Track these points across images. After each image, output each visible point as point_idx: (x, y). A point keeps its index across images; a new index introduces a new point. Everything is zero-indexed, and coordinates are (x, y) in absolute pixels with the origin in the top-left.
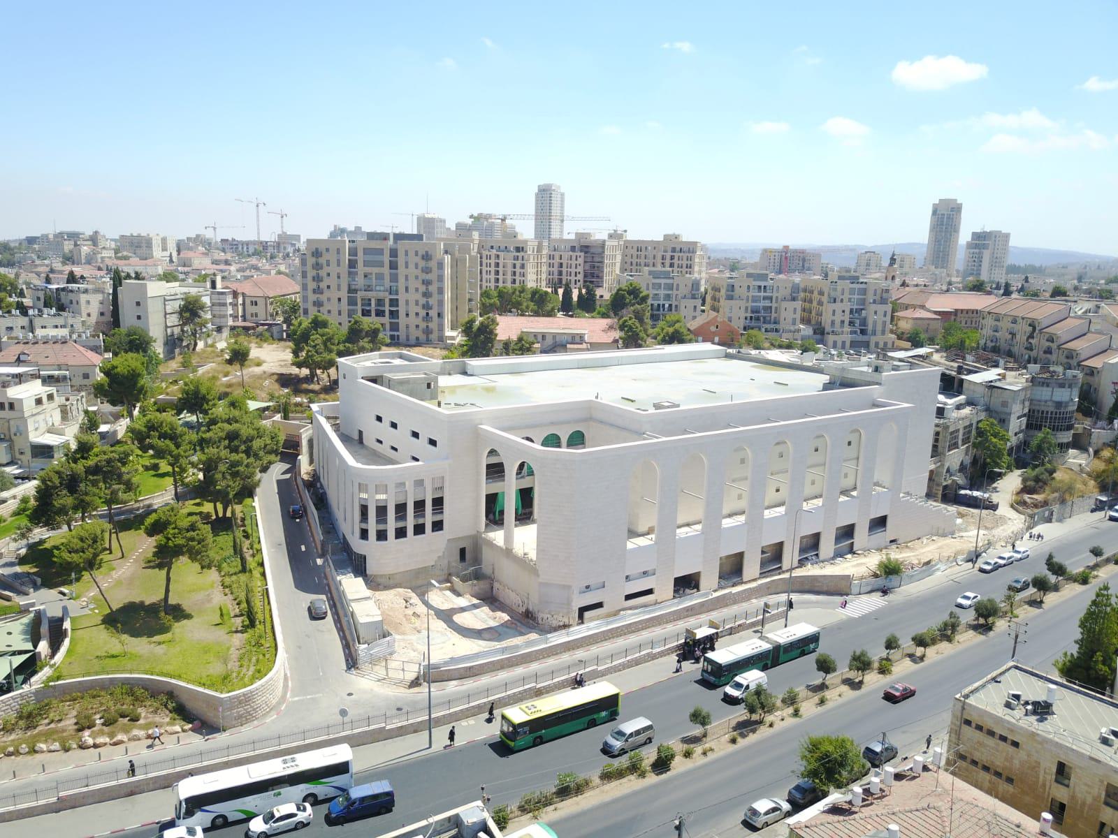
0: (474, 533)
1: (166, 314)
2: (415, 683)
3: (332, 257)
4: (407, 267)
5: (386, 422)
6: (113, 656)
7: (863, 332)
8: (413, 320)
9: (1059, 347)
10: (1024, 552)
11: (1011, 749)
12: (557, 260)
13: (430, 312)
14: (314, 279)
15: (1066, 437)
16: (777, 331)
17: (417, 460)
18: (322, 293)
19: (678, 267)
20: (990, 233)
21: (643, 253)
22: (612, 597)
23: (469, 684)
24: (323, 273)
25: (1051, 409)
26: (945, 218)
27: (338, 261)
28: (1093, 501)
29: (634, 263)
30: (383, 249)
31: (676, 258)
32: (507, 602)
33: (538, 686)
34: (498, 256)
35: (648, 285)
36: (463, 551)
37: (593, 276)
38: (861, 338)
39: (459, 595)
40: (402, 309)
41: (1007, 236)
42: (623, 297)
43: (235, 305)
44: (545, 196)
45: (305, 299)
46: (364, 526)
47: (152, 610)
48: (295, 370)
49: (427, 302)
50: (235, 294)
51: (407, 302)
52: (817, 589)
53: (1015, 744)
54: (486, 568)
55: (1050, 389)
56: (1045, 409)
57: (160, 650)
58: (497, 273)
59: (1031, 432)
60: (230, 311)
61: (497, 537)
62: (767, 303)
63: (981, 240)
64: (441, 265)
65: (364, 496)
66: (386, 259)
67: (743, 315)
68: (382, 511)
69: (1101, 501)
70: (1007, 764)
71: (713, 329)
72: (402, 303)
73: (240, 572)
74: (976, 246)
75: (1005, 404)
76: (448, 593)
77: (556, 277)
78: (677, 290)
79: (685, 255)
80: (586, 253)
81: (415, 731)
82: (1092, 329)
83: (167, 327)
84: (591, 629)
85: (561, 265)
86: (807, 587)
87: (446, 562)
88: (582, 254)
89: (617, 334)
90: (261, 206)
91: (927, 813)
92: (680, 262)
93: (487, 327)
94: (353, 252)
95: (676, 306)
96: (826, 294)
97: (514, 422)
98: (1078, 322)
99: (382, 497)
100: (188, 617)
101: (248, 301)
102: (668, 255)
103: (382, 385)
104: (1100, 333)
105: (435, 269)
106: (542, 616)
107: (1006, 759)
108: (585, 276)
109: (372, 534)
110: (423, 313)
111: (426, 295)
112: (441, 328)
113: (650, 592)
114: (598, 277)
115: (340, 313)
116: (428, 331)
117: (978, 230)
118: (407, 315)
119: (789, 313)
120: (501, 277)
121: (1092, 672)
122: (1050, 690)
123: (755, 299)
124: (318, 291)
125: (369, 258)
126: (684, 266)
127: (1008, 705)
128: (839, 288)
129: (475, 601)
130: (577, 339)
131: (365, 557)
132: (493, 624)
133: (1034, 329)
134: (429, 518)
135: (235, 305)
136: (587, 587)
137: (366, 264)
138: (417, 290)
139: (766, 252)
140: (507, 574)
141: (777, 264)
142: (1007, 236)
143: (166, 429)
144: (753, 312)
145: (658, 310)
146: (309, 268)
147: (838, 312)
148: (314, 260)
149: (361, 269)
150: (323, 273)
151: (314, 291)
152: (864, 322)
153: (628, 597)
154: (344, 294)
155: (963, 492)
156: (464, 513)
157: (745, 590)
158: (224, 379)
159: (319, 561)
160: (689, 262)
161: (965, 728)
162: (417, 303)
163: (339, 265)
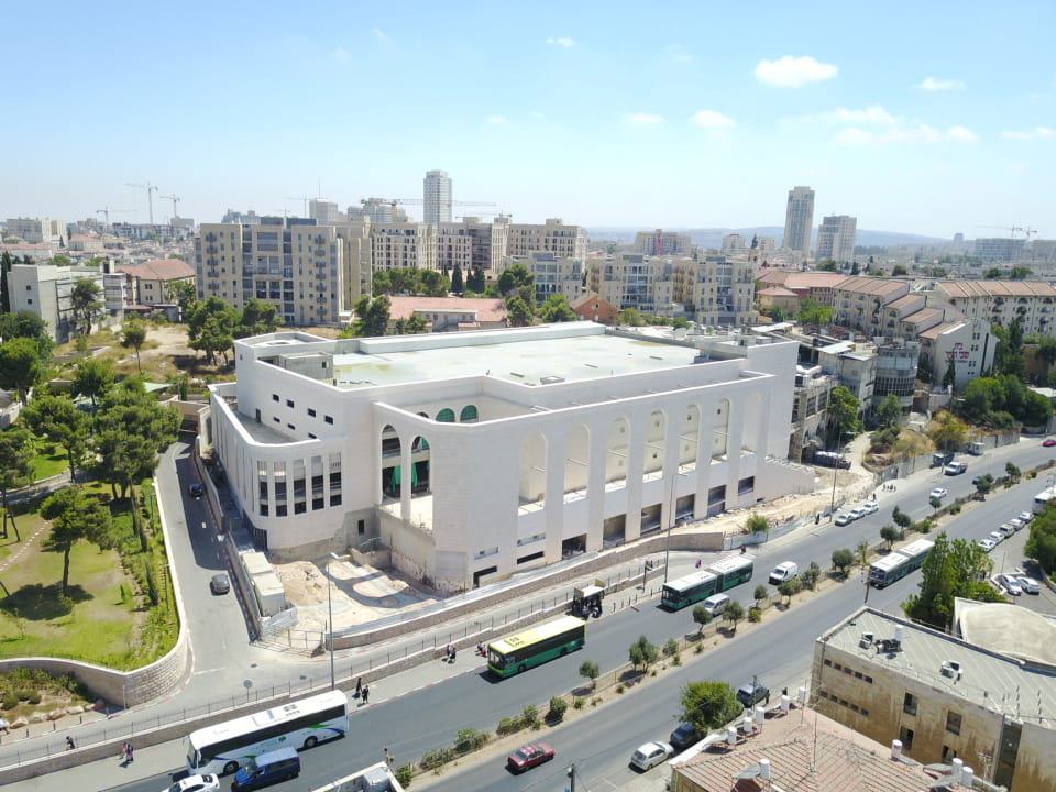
0: (372, 506)
2: (318, 652)
3: (227, 241)
4: (301, 250)
5: (283, 401)
6: (11, 640)
7: (730, 309)
8: (307, 302)
9: (900, 321)
11: (866, 685)
12: (446, 243)
13: (325, 294)
14: (208, 262)
15: (908, 401)
16: (652, 309)
17: (314, 437)
18: (217, 276)
20: (840, 218)
21: (527, 237)
22: (506, 562)
23: (371, 650)
24: (218, 257)
25: (895, 377)
26: (800, 203)
28: (931, 458)
30: (276, 234)
31: (558, 241)
32: (406, 570)
36: (361, 524)
37: (481, 259)
38: (727, 314)
39: (358, 565)
40: (296, 292)
41: (854, 221)
42: (510, 278)
43: (129, 289)
44: (434, 182)
45: (200, 283)
46: (264, 502)
47: (51, 592)
48: (192, 352)
49: (321, 284)
50: (129, 278)
51: (301, 284)
52: (694, 547)
53: (869, 680)
54: (384, 539)
55: (893, 359)
56: (890, 377)
57: (59, 632)
58: (389, 255)
59: (878, 398)
60: (124, 294)
61: (395, 509)
62: (642, 283)
63: (832, 224)
64: (334, 249)
65: (263, 473)
66: (280, 243)
67: (620, 294)
68: (281, 487)
69: (938, 458)
70: (862, 698)
71: (594, 308)
73: (141, 551)
74: (828, 229)
75: (855, 373)
76: (348, 564)
77: (446, 259)
80: (474, 236)
82: (929, 303)
85: (450, 248)
86: (684, 545)
87: (344, 538)
88: (470, 238)
89: (505, 313)
90: (154, 191)
91: (794, 747)
93: (380, 307)
94: (247, 236)
96: (696, 273)
97: (410, 398)
98: (915, 298)
99: (282, 474)
100: (89, 597)
101: (142, 285)
102: (551, 238)
103: (278, 365)
104: (935, 307)
106: (440, 582)
107: (862, 693)
108: (474, 258)
109: (272, 510)
111: (320, 276)
112: (335, 309)
113: (540, 555)
114: (486, 259)
115: (235, 295)
116: (322, 312)
117: (829, 215)
118: (302, 296)
119: (662, 291)
120: (392, 259)
121: (933, 612)
122: (898, 630)
123: (632, 280)
124: (213, 274)
125: (264, 242)
126: (566, 249)
127: (862, 645)
128: (708, 269)
129: (375, 571)
130: (468, 318)
131: (266, 532)
132: (392, 592)
133: (879, 306)
134: (327, 493)
135: (129, 289)
136: (482, 553)
137: (260, 248)
138: (311, 272)
139: (640, 234)
140: (404, 545)
141: (651, 246)
142: (854, 221)
143: (61, 412)
144: (629, 291)
145: (543, 290)
146: (203, 251)
147: (708, 291)
148: (208, 244)
149: (255, 252)
150: (218, 257)
151: (209, 275)
152: (730, 300)
153: (520, 561)
154: (239, 277)
155: (820, 453)
156: (362, 488)
158: (120, 362)
159: (220, 538)
160: (570, 245)
161: (826, 668)
162: (311, 285)
163: (233, 249)
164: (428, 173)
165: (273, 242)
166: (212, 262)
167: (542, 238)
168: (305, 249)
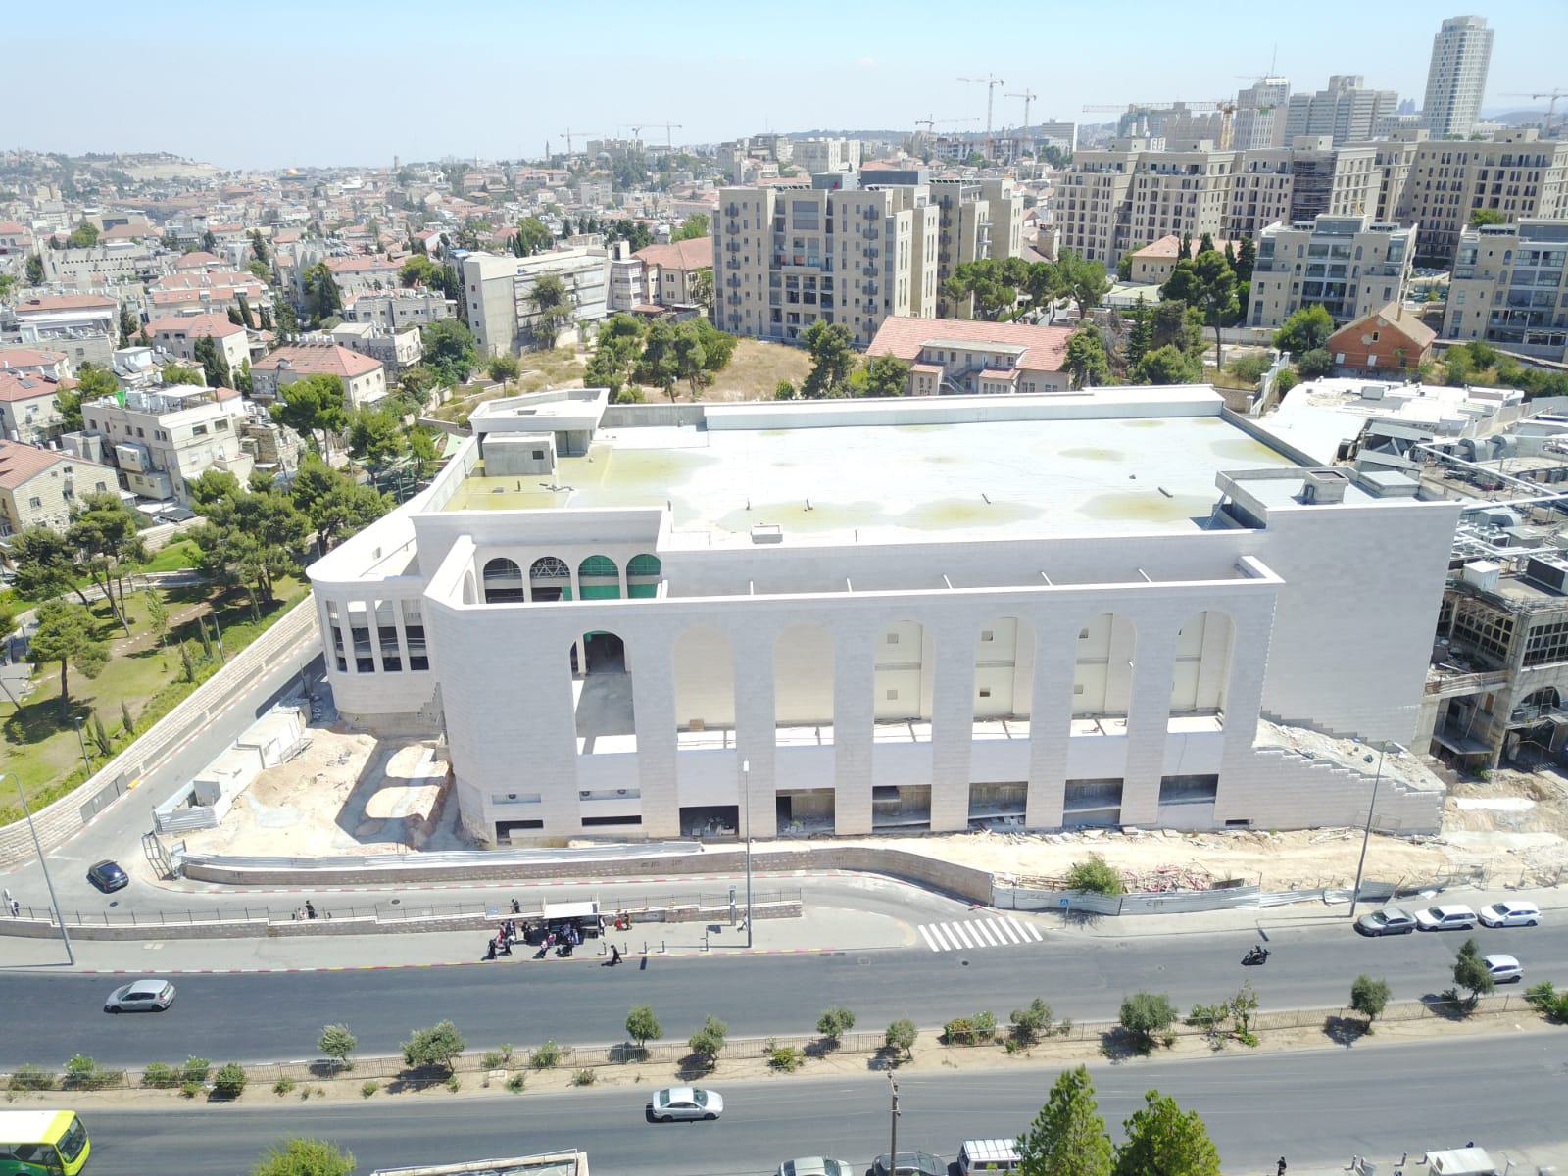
1: (516, 300)
4: (845, 230)
8: (852, 311)
10: (1513, 914)
12: (1250, 187)
13: (874, 298)
18: (738, 268)
19: (1509, 193)
21: (1452, 166)
22: (562, 814)
24: (739, 239)
27: (758, 220)
29: (1434, 185)
31: (1507, 176)
33: (273, 924)
34: (1156, 182)
35: (1301, 248)
43: (643, 281)
45: (719, 273)
49: (871, 284)
50: (645, 266)
52: (933, 880)
60: (635, 288)
64: (890, 225)
67: (1486, 308)
71: (1367, 340)
72: (837, 284)
73: (185, 681)
77: (1244, 217)
78: (1358, 257)
79: (1524, 170)
81: (91, 938)
83: (517, 317)
84: (448, 860)
85: (1254, 196)
86: (917, 873)
92: (1514, 184)
95: (1353, 288)
102: (1492, 171)
105: (882, 233)
110: (864, 300)
111: (870, 272)
113: (636, 820)
118: (844, 301)
120: (1158, 216)
123: (1520, 278)
124: (734, 264)
126: (1522, 190)
130: (1004, 363)
135: (643, 281)
138: (857, 264)
145: (1342, 294)
148: (729, 219)
149: (790, 233)
153: (587, 822)
154: (765, 269)
157: (779, 855)
163: (758, 227)
164: (1444, 22)
165: (811, 215)
166: (733, 247)
167: (1474, 168)
168: (851, 228)
